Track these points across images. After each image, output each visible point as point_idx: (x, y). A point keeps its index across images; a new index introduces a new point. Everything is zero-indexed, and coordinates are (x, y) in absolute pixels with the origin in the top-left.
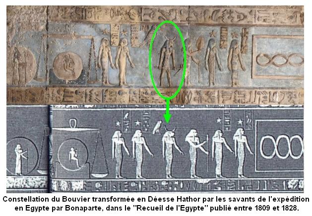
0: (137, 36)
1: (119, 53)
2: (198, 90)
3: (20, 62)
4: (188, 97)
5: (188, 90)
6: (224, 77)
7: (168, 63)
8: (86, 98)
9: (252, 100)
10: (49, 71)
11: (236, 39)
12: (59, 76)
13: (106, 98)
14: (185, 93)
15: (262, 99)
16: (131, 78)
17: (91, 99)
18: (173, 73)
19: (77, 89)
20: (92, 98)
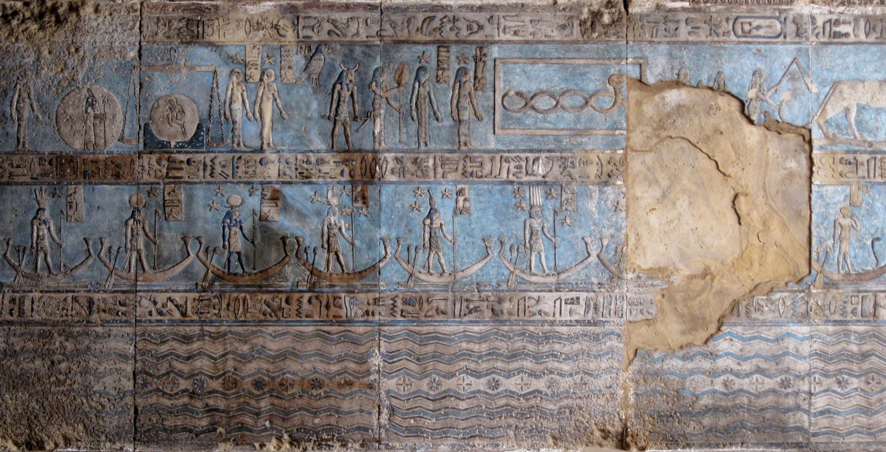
0: (291, 64)
1: (260, 94)
2: (400, 155)
3: (96, 112)
4: (381, 168)
5: (382, 156)
6: (444, 133)
7: (345, 110)
8: (205, 170)
9: (496, 171)
10: (142, 126)
11: (465, 65)
12: (160, 134)
13: (239, 171)
14: (376, 161)
15: (513, 170)
16: (280, 135)
17: (212, 173)
18: (354, 128)
19: (189, 156)
20: (215, 171)
